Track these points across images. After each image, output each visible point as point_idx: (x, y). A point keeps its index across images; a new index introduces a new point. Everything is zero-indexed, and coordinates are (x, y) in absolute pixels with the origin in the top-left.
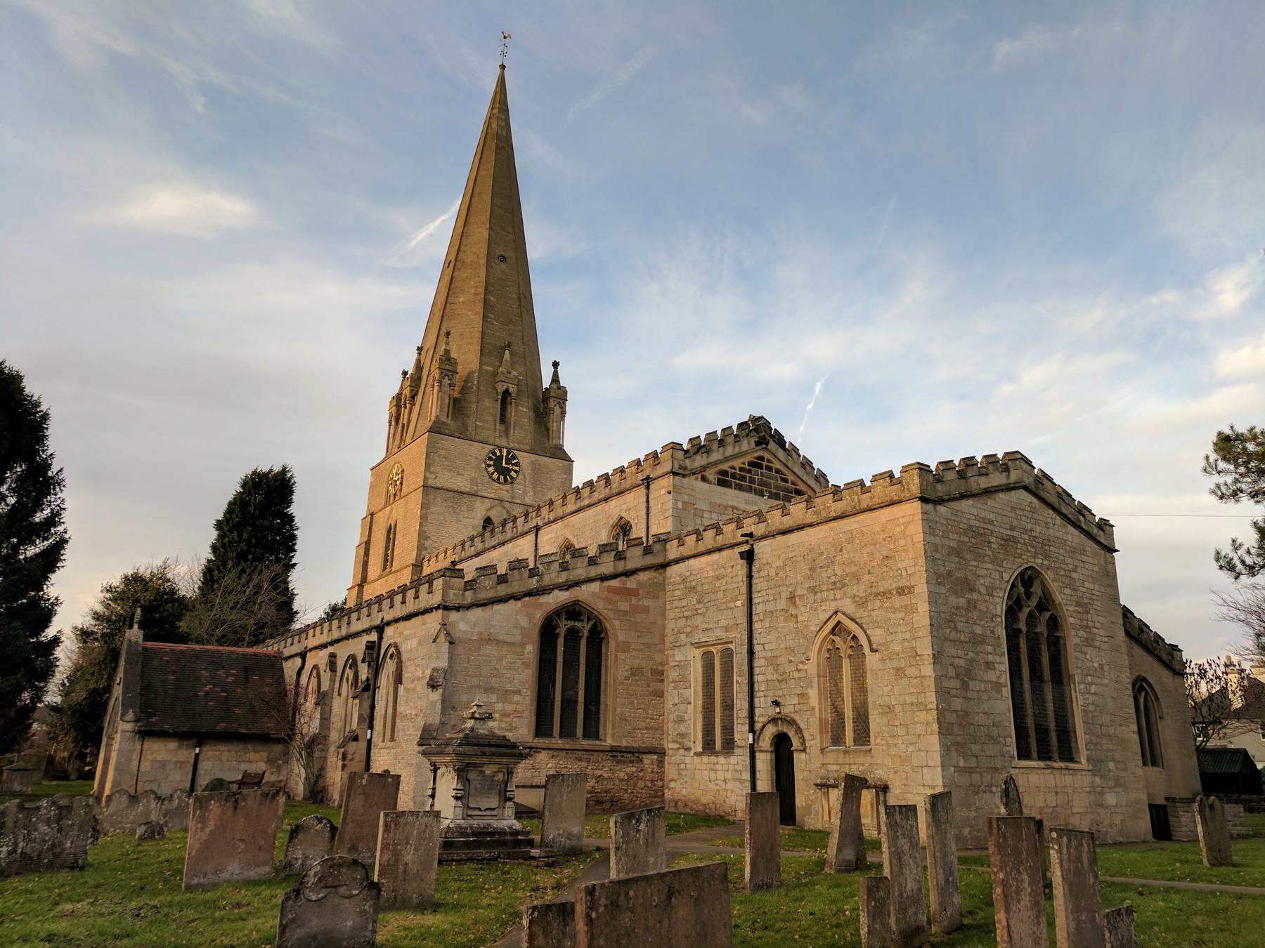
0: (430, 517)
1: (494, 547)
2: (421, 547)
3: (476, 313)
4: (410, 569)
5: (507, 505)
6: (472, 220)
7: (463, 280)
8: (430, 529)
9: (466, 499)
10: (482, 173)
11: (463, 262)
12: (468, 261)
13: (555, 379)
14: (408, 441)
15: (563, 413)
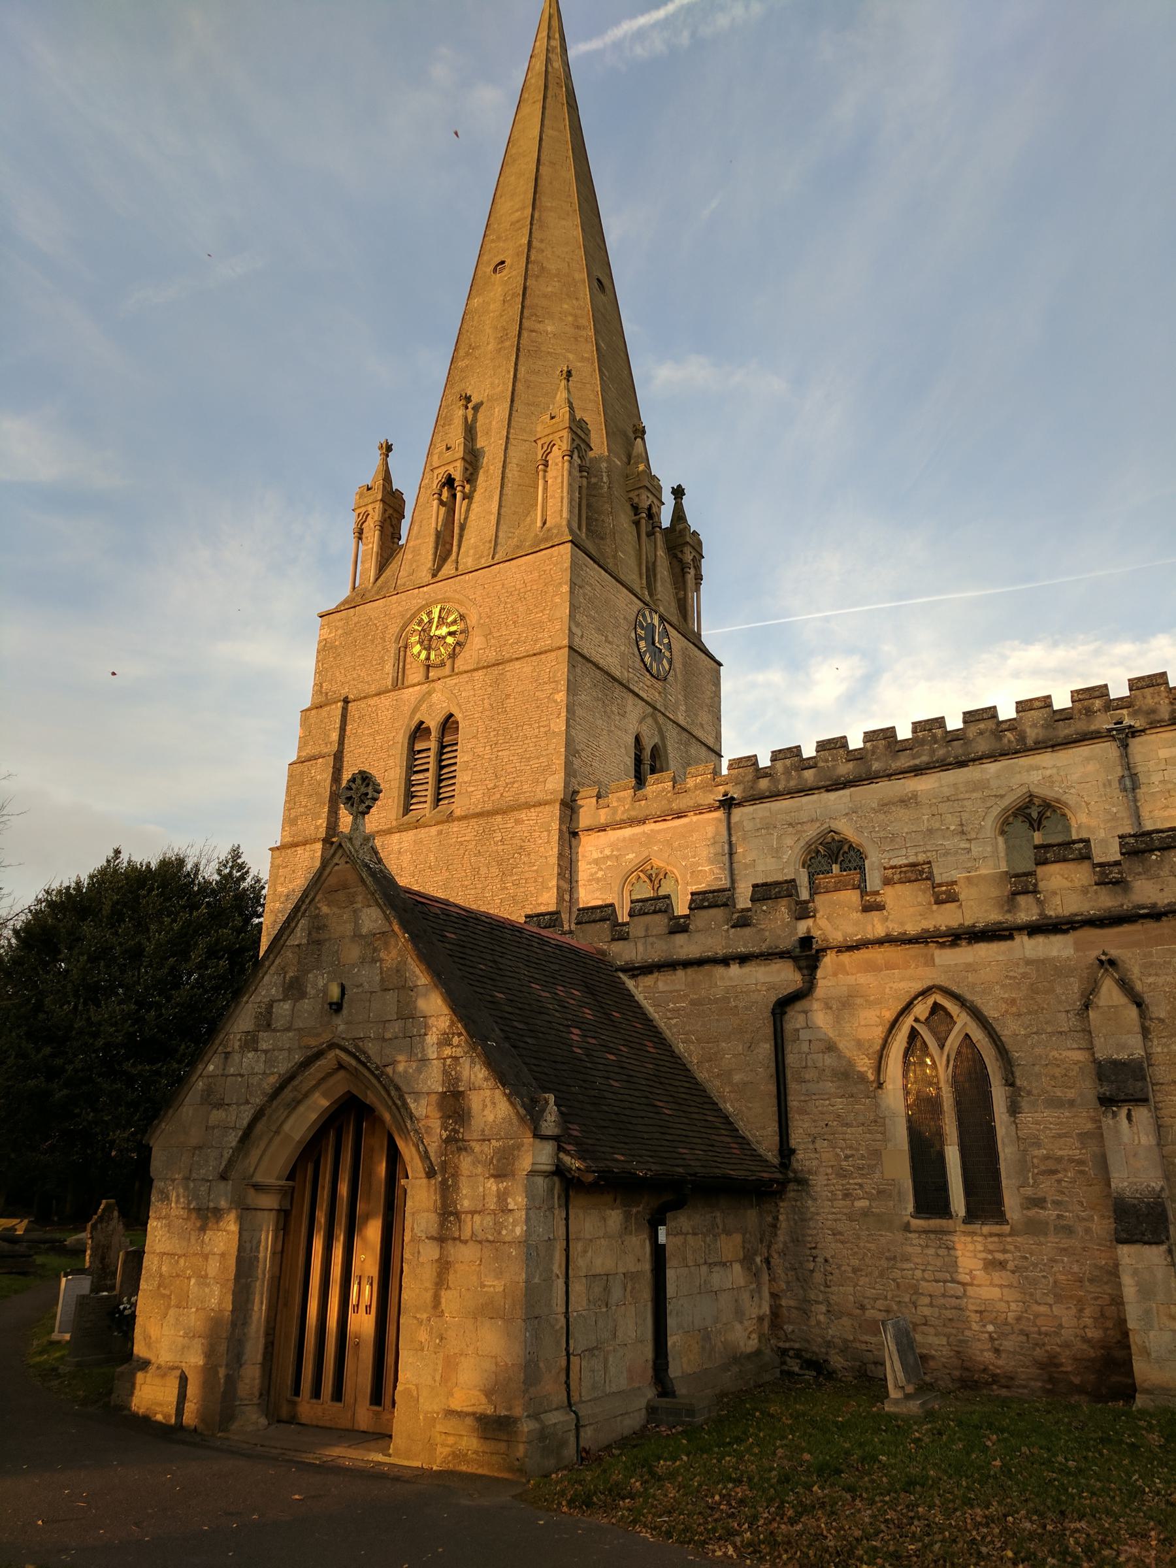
0: (579, 712)
1: (918, 771)
2: (570, 771)
3: (583, 359)
4: (557, 806)
5: (661, 719)
6: (545, 201)
7: (545, 296)
8: (580, 736)
9: (618, 691)
10: (548, 132)
11: (543, 268)
12: (552, 267)
13: (679, 515)
14: (467, 561)
15: (699, 578)
